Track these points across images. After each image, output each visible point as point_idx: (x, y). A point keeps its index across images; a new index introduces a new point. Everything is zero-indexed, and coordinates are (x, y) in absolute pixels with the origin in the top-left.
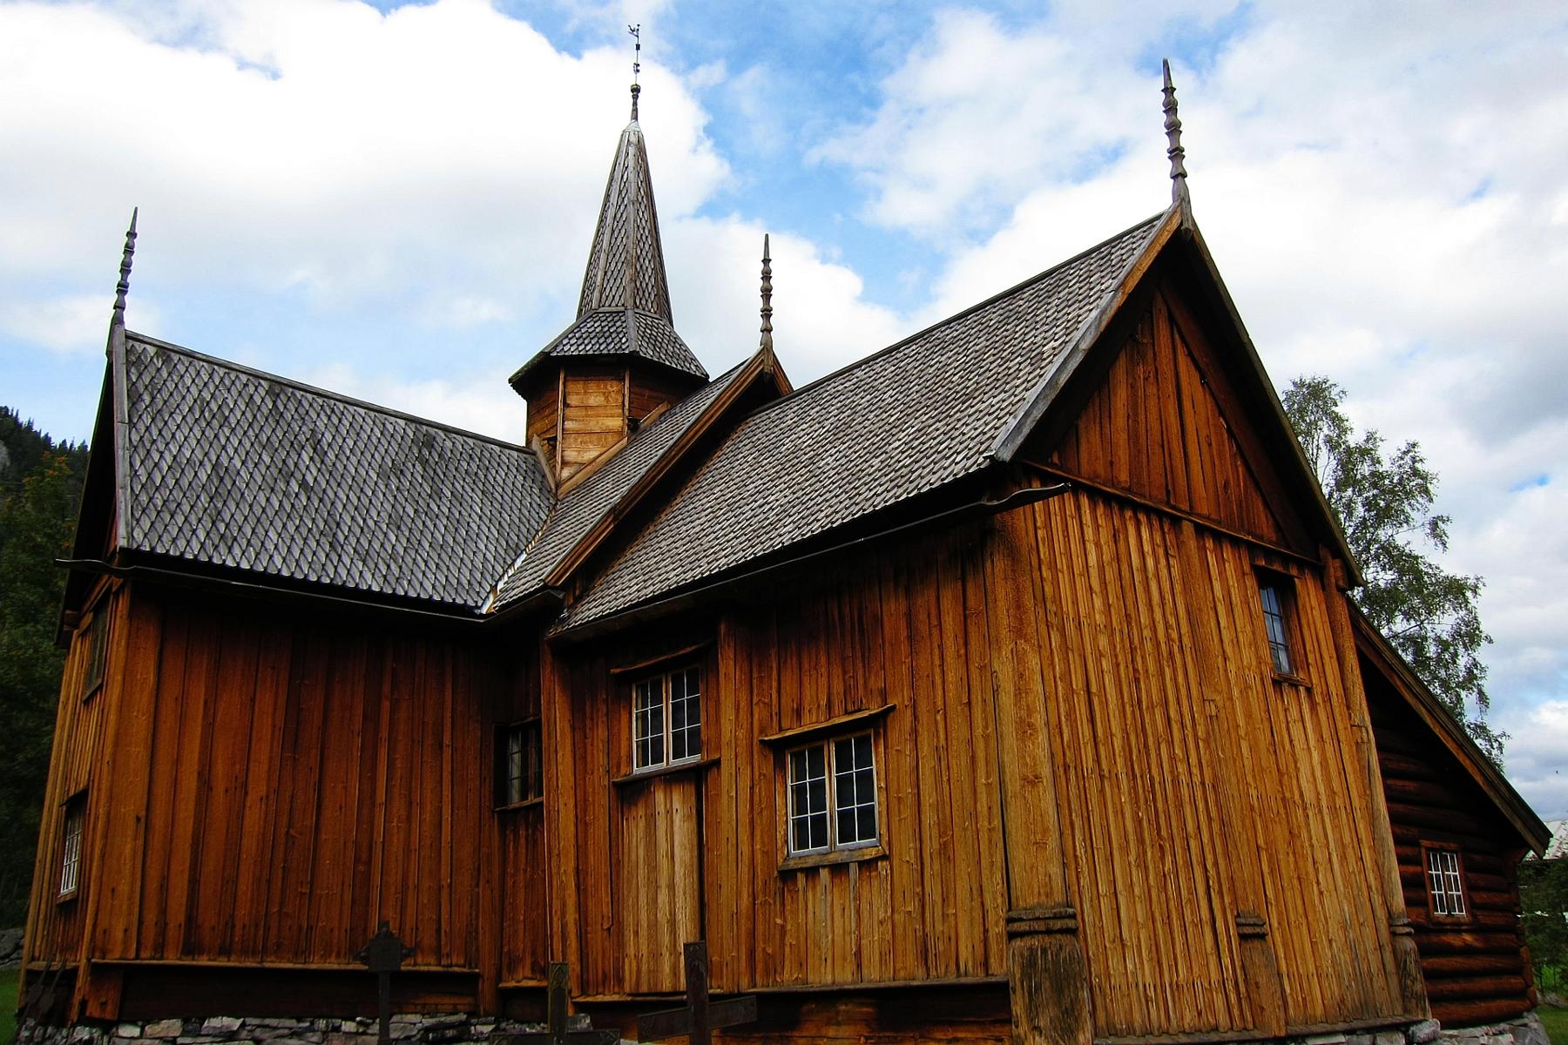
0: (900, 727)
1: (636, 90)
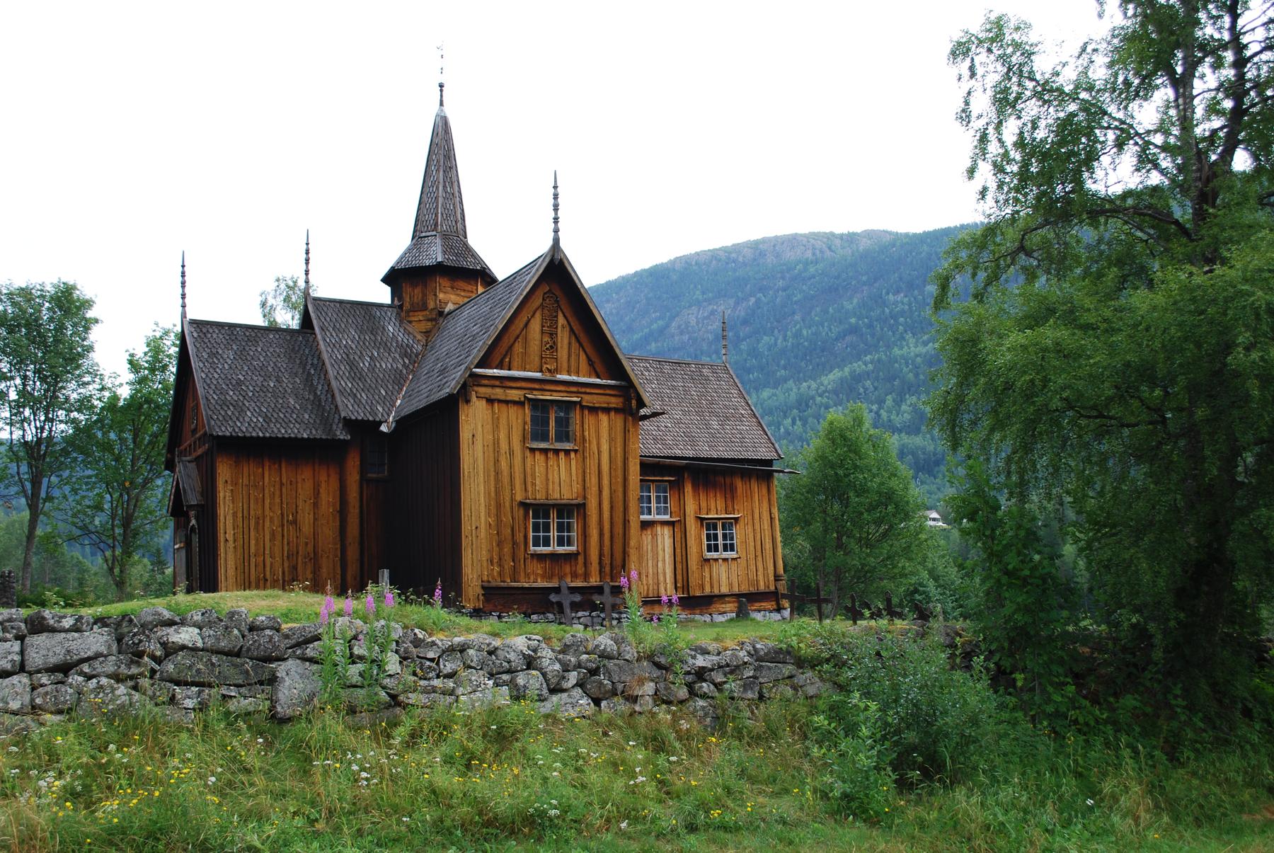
0: (741, 522)
1: (441, 86)
